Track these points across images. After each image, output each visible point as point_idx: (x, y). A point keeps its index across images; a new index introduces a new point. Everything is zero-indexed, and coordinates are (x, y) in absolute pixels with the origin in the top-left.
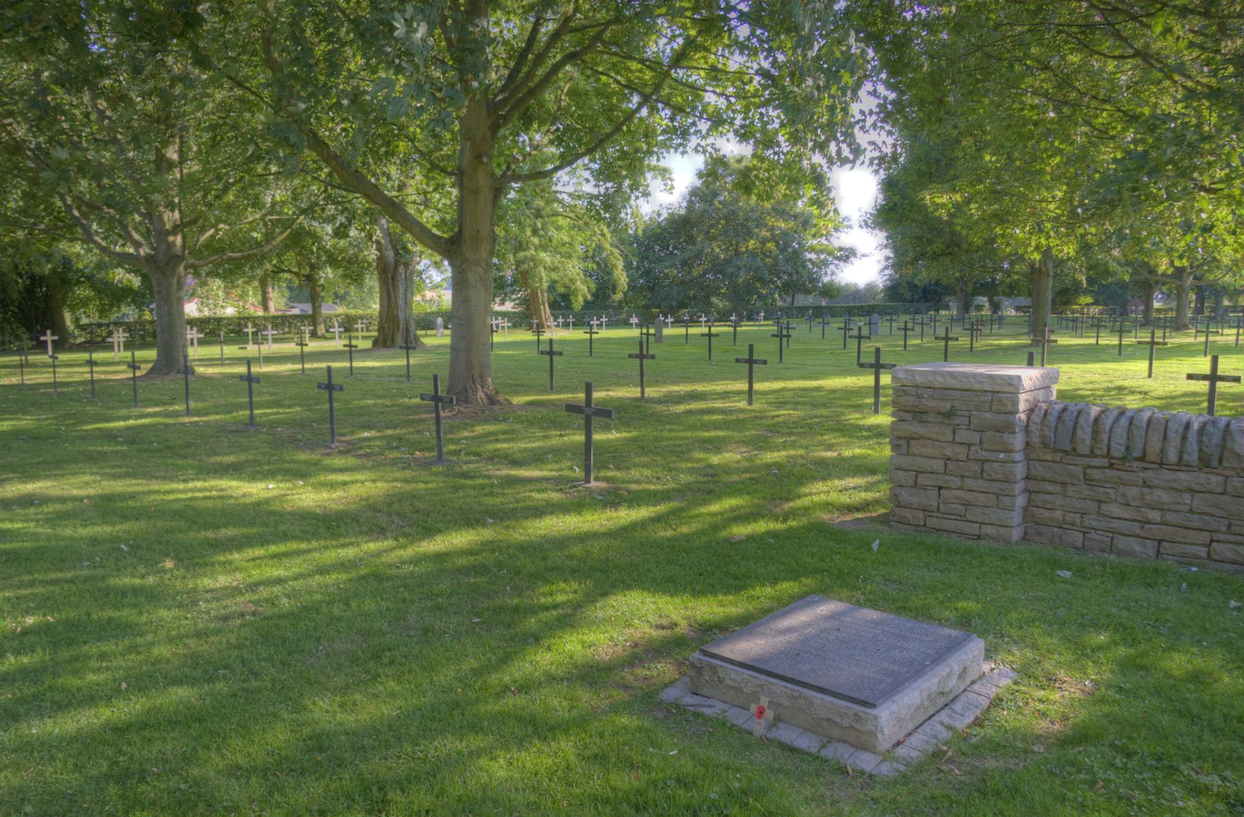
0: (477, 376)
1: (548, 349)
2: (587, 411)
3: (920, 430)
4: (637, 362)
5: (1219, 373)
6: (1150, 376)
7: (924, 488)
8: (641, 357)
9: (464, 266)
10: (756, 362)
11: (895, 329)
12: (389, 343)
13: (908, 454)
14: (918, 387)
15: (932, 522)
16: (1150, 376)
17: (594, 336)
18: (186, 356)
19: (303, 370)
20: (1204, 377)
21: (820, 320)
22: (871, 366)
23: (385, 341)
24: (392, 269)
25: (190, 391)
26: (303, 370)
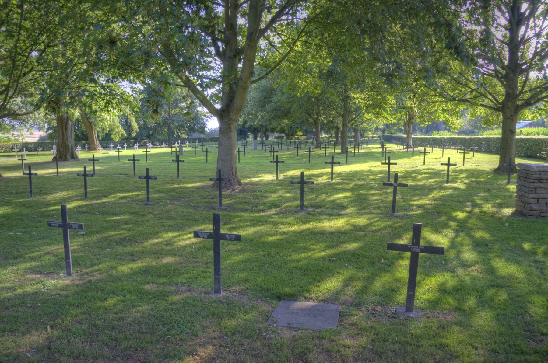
0: (234, 173)
1: (132, 159)
2: (395, 185)
3: (541, 185)
4: (275, 164)
5: (447, 163)
6: (424, 164)
7: (541, 204)
8: (178, 161)
9: (230, 122)
10: (180, 161)
11: (267, 149)
12: (63, 158)
13: (535, 193)
14: (541, 171)
15: (542, 214)
16: (424, 164)
17: (121, 154)
18: (236, 168)
19: (58, 173)
20: (446, 164)
21: (201, 144)
22: (330, 163)
23: (61, 158)
24: (65, 121)
25: (84, 188)
26: (58, 173)
